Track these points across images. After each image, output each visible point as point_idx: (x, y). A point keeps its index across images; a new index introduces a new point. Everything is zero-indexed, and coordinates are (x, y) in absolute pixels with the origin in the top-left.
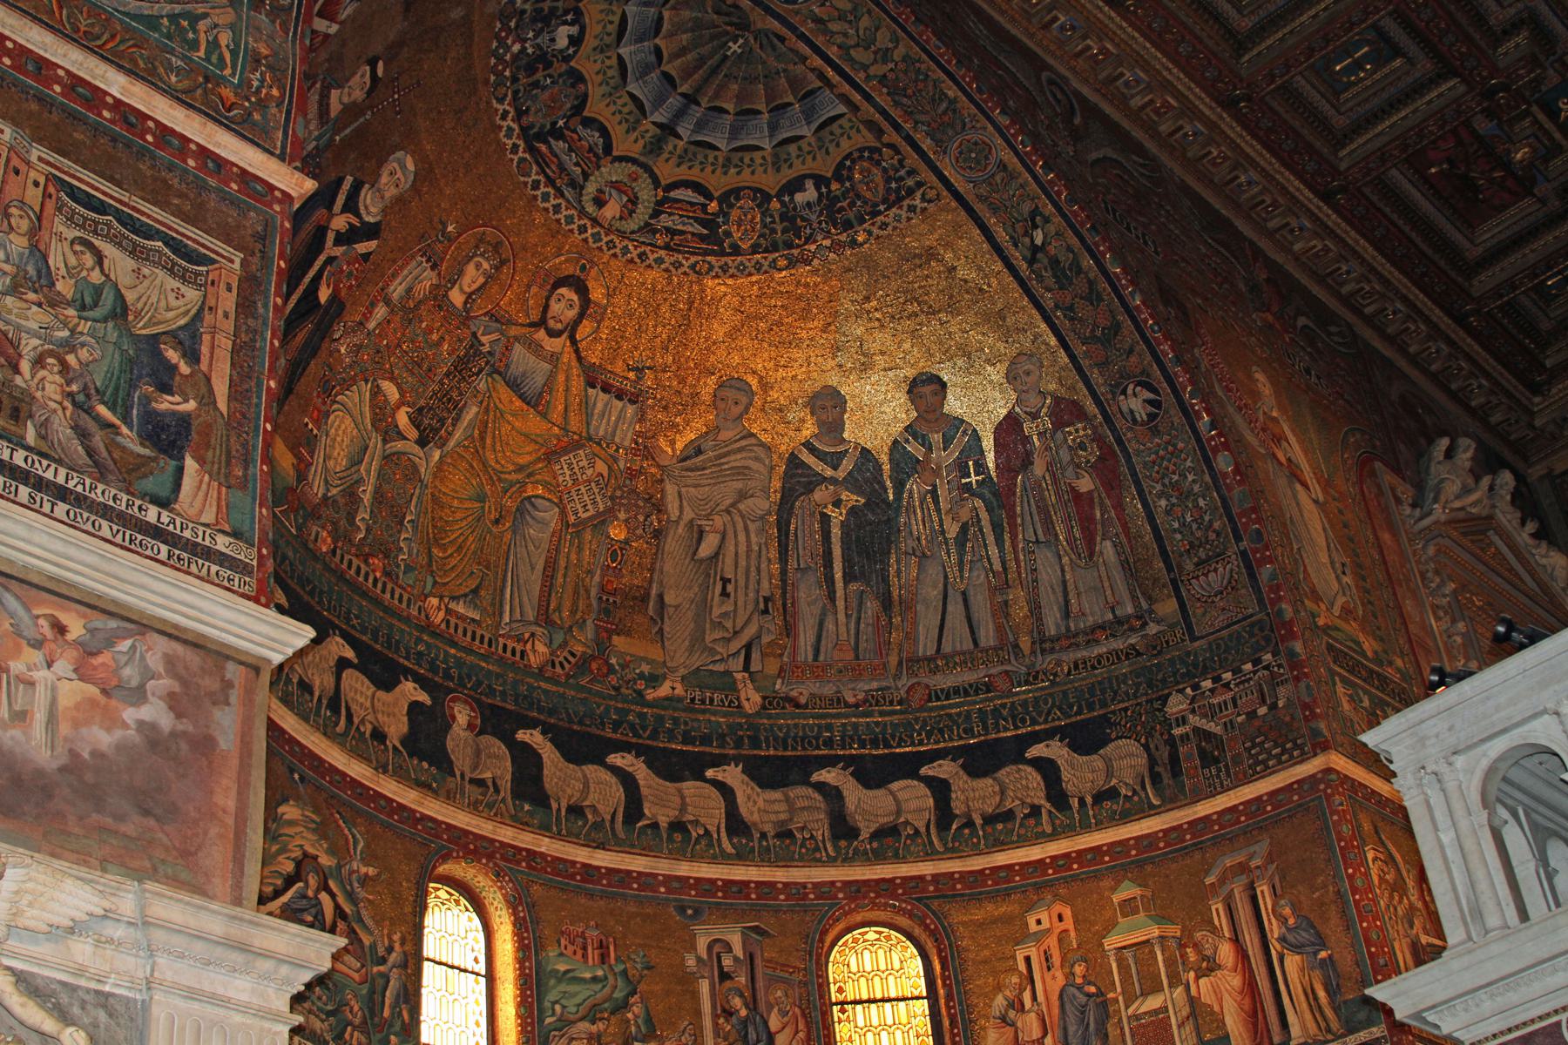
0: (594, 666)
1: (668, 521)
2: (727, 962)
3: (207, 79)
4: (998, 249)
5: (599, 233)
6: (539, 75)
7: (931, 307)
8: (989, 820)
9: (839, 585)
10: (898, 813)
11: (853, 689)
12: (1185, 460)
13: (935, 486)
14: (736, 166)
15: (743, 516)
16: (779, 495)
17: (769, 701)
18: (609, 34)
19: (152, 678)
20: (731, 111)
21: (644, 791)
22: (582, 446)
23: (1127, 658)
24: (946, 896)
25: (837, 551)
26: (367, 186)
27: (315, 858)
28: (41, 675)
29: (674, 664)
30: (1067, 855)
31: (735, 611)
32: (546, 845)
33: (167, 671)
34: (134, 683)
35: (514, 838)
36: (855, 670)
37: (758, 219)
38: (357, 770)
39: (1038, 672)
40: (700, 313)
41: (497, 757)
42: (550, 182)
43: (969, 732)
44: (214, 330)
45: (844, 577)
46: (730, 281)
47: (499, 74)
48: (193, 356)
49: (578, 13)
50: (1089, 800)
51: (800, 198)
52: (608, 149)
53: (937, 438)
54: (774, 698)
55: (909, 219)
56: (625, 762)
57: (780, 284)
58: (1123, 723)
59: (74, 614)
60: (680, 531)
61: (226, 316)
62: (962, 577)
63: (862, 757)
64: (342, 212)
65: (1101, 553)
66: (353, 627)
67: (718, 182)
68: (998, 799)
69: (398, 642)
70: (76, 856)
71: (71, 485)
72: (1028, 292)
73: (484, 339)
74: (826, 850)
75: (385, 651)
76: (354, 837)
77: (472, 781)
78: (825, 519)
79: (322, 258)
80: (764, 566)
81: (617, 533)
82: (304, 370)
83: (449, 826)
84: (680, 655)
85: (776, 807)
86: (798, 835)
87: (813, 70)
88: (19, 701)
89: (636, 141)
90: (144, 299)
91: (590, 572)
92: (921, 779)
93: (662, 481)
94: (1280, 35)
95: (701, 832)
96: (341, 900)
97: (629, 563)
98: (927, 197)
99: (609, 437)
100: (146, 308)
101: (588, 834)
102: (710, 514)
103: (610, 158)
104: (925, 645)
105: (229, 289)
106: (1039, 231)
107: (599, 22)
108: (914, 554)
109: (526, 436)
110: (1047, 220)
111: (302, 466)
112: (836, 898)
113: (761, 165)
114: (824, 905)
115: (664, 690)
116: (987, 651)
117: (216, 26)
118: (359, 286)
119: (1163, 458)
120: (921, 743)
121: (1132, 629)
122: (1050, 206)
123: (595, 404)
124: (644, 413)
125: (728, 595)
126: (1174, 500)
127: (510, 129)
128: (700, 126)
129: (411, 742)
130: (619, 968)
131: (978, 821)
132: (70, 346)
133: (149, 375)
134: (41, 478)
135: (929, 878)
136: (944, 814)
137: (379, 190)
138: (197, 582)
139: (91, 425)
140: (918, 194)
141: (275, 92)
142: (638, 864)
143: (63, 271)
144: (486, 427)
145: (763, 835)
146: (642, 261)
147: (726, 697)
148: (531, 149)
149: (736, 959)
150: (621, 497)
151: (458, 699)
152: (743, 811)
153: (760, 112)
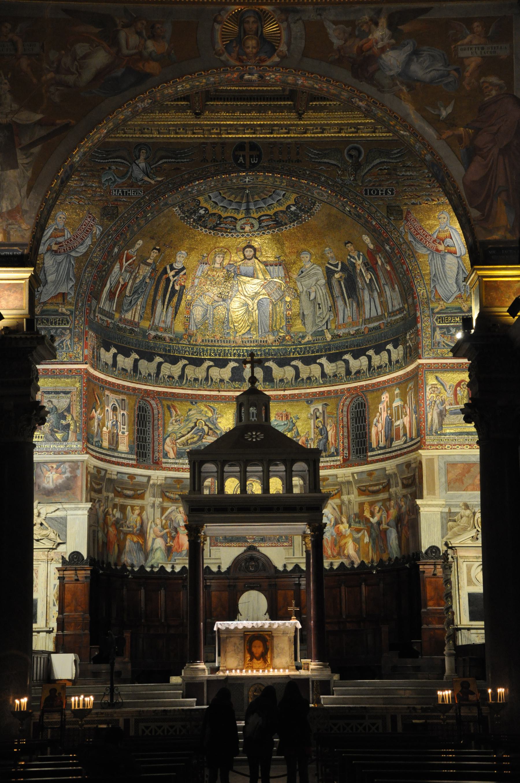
0: (287, 338)
2: (318, 414)
10: (361, 366)
21: (300, 370)
52: (236, 219)
53: (356, 257)
64: (171, 271)
67: (271, 212)
69: (227, 353)
78: (339, 282)
79: (171, 283)
80: (328, 298)
81: (288, 299)
84: (310, 329)
96: (210, 426)
128: (255, 205)
129: (233, 379)
130: (291, 421)
145: (330, 377)
148: (216, 230)
149: (320, 413)
152: (325, 371)
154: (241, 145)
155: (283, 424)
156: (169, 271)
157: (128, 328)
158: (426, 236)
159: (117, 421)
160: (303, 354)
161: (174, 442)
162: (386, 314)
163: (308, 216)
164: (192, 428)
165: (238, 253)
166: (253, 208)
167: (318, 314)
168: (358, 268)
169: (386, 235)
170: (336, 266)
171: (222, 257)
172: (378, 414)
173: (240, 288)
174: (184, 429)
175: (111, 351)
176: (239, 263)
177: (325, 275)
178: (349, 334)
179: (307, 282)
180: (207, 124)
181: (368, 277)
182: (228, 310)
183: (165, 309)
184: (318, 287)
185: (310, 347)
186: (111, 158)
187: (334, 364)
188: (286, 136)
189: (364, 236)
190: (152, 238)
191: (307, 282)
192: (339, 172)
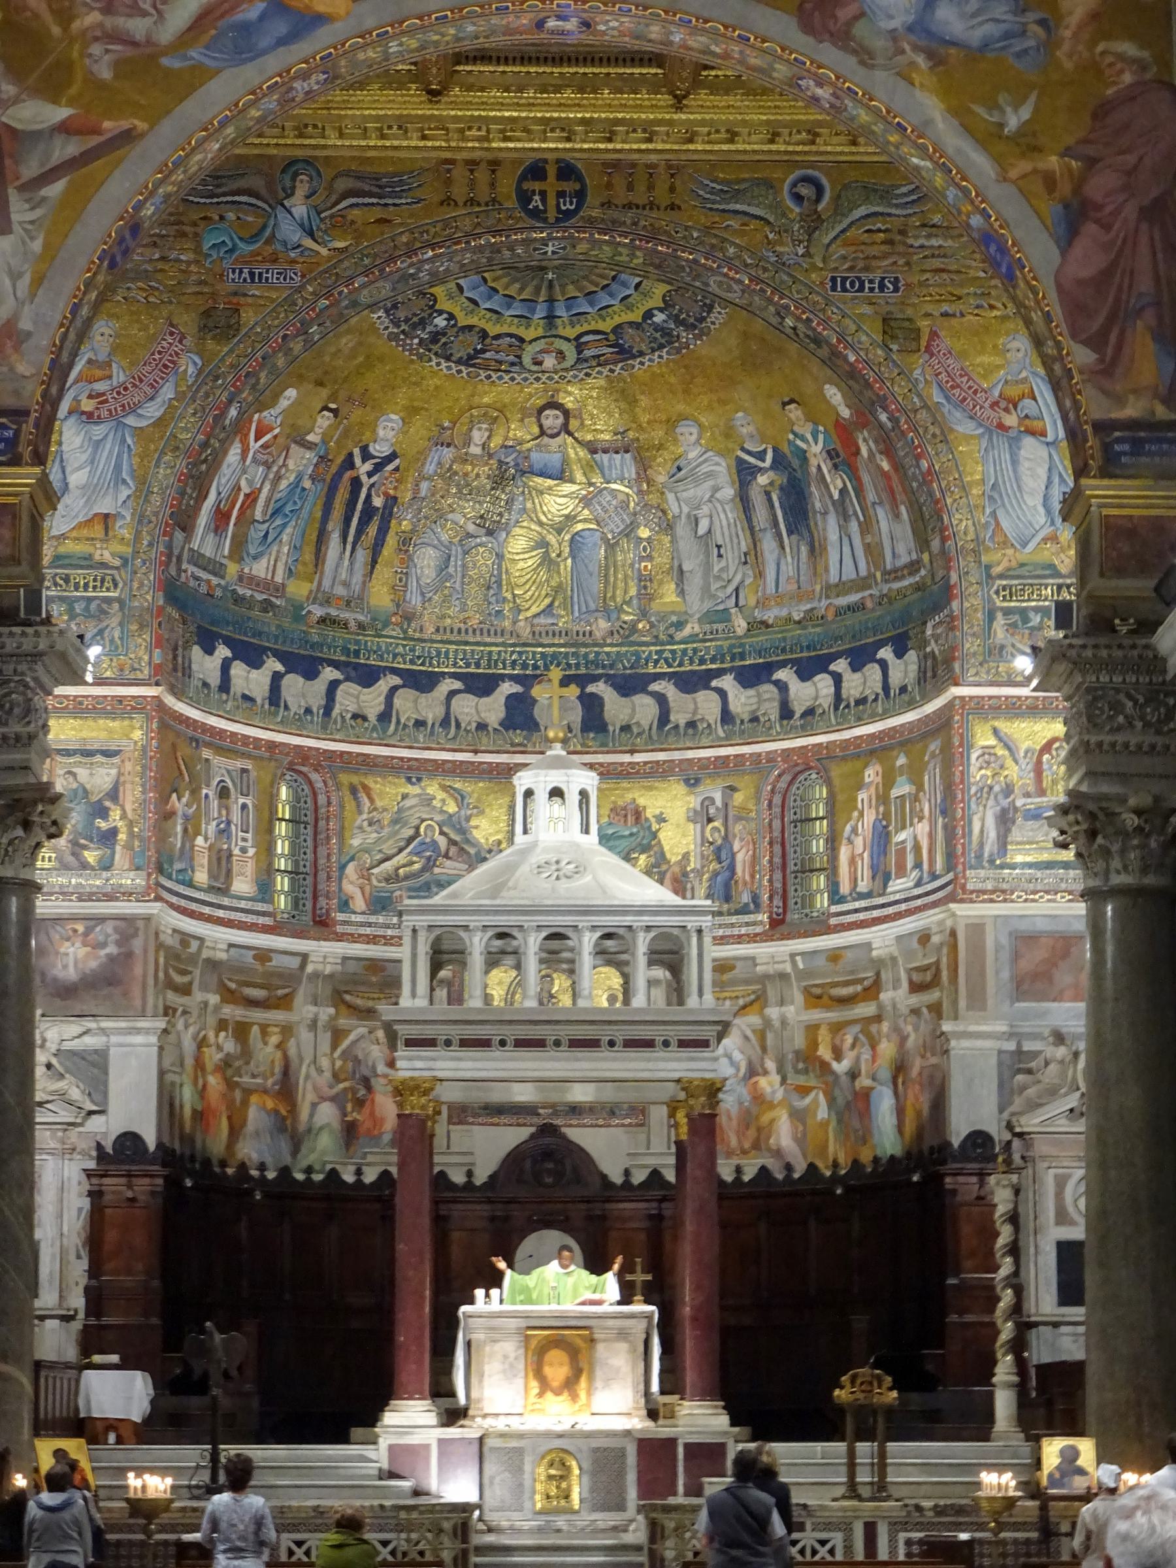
2: (712, 811)
10: (816, 698)
21: (672, 704)
36: (800, 595)
52: (522, 340)
64: (364, 461)
67: (607, 326)
78: (768, 494)
81: (644, 533)
84: (696, 605)
96: (453, 836)
128: (568, 308)
129: (508, 724)
145: (742, 722)
148: (473, 366)
154: (536, 171)
155: (627, 833)
156: (358, 461)
157: (260, 597)
158: (975, 392)
159: (229, 823)
160: (680, 665)
161: (365, 874)
162: (878, 575)
163: (696, 337)
164: (410, 840)
166: (564, 314)
167: (716, 569)
168: (814, 462)
169: (880, 388)
170: (761, 456)
172: (856, 814)
173: (529, 505)
174: (391, 842)
175: (217, 653)
176: (529, 445)
177: (735, 477)
178: (789, 619)
179: (690, 493)
180: (455, 116)
181: (836, 483)
182: (500, 556)
183: (348, 553)
185: (695, 650)
186: (224, 194)
187: (751, 692)
188: (643, 146)
189: (827, 386)
190: (320, 383)
191: (690, 493)
192: (771, 236)
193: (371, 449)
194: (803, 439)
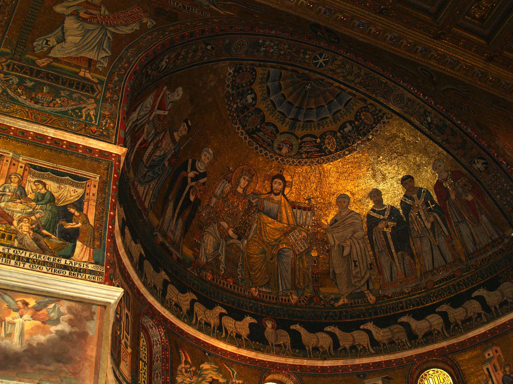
0: (315, 299)
1: (331, 246)
3: (86, 126)
4: (417, 127)
5: (283, 158)
6: (246, 113)
7: (401, 153)
8: (463, 322)
9: (394, 254)
10: (431, 326)
11: (407, 288)
12: (502, 179)
13: (419, 212)
14: (322, 125)
15: (356, 239)
16: (367, 229)
17: (378, 298)
18: (265, 94)
19: (63, 315)
20: (314, 108)
21: (339, 337)
22: (296, 229)
23: (500, 253)
24: (454, 352)
25: (391, 243)
26: (197, 161)
27: (218, 380)
28: (18, 321)
29: (343, 293)
30: (494, 328)
31: (360, 271)
32: (306, 362)
33: (68, 312)
34: (55, 318)
35: (294, 362)
37: (334, 140)
38: (231, 348)
39: (470, 267)
40: (324, 176)
41: (284, 336)
42: (261, 146)
43: (450, 293)
44: (88, 201)
45: (395, 251)
46: (331, 163)
47: (232, 116)
48: (80, 209)
49: (252, 90)
50: (497, 306)
51: (346, 130)
52: (277, 131)
53: (415, 196)
54: (380, 297)
55: (384, 126)
56: (331, 329)
57: (348, 160)
58: (504, 277)
59: (32, 298)
60: (336, 248)
61: (94, 195)
62: (436, 240)
63: (414, 310)
64: (191, 171)
65: (482, 220)
66: (225, 302)
67: (317, 132)
68: (465, 314)
70: (29, 380)
71: (31, 257)
72: (431, 138)
73: (253, 201)
74: (407, 345)
75: (239, 308)
76: (232, 371)
77: (276, 345)
78: (385, 233)
79: (188, 187)
80: (367, 253)
81: (314, 254)
82: (191, 223)
83: (269, 362)
84: (344, 289)
85: (387, 334)
86: (397, 342)
87: (337, 87)
88: (9, 330)
89: (286, 126)
90: (62, 195)
91: (308, 269)
92: (437, 313)
93: (326, 234)
94: (500, 31)
95: (362, 348)
97: (320, 263)
98: (388, 117)
99: (304, 223)
100: (62, 198)
101: (321, 356)
102: (345, 240)
103: (279, 134)
104: (429, 267)
105: (95, 186)
106: (429, 117)
107: (260, 91)
108: (417, 237)
109: (275, 229)
110: (430, 113)
111: (196, 254)
112: (414, 361)
113: (330, 123)
114: (410, 364)
115: (341, 302)
116: (450, 263)
117: (89, 109)
118: (204, 193)
119: (494, 181)
120: (434, 301)
121: (499, 243)
122: (429, 108)
123: (297, 214)
124: (314, 213)
125: (357, 266)
126: (502, 194)
127: (242, 133)
128: (306, 116)
131: (460, 323)
132: (32, 214)
133: (63, 218)
134: (20, 256)
135: (446, 347)
136: (447, 323)
137: (202, 162)
138: (98, 284)
139: (39, 236)
140: (385, 117)
141: (112, 125)
142: (340, 363)
143: (31, 191)
144: (261, 229)
145: (384, 344)
146: (300, 164)
147: (363, 300)
150: (313, 242)
151: (267, 319)
152: (376, 337)
153: (324, 106)
165: (266, 182)
167: (354, 272)
171: (247, 180)
176: (264, 196)
184: (355, 240)
193: (197, 163)
194: (411, 198)
